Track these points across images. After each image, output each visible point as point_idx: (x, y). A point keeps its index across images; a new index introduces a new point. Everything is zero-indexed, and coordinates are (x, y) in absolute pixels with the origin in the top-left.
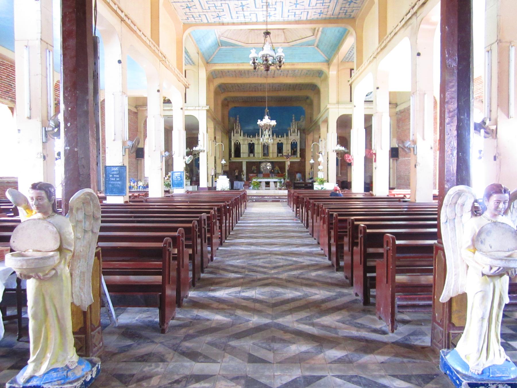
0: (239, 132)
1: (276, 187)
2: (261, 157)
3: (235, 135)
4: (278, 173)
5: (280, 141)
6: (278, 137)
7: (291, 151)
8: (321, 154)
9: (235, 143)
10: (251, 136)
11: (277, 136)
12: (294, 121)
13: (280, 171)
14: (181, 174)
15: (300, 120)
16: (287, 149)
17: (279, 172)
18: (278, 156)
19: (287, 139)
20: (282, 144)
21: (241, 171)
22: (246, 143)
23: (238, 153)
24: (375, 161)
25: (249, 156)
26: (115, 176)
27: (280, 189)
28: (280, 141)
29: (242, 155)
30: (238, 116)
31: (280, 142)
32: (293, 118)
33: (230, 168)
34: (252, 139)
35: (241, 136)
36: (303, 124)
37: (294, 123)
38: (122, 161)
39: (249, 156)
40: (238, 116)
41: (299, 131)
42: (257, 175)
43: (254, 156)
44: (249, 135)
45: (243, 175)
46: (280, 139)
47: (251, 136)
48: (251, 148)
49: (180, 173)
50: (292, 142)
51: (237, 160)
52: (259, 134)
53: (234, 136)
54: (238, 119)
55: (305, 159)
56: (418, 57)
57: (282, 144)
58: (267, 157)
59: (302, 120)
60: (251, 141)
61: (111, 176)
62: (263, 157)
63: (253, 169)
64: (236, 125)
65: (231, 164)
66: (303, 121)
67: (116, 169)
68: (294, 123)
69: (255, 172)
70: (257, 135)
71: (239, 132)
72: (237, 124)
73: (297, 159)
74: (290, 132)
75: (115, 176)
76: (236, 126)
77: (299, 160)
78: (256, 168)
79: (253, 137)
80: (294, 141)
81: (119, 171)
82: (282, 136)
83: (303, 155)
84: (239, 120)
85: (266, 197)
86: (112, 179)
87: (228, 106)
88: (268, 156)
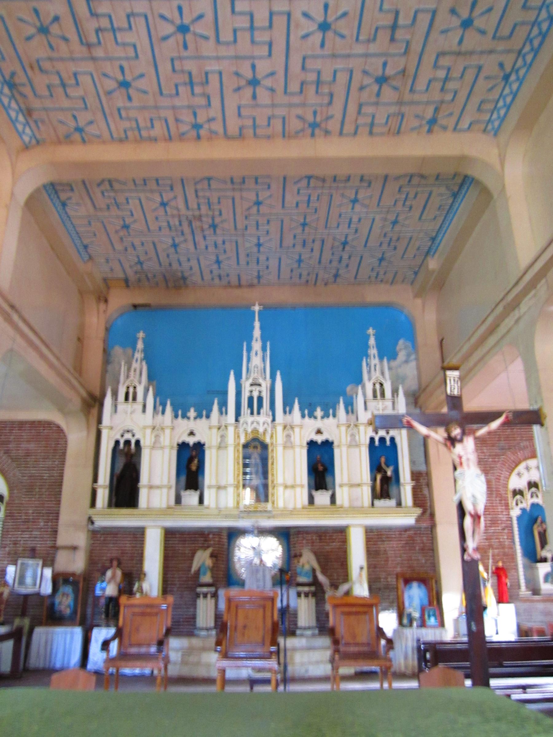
2: (231, 503)
3: (120, 407)
4: (315, 582)
5: (319, 432)
6: (312, 415)
7: (374, 479)
9: (117, 443)
10: (192, 413)
12: (373, 351)
13: (324, 572)
17: (321, 578)
20: (328, 445)
25: (178, 500)
28: (319, 432)
30: (141, 335)
31: (319, 439)
32: (372, 341)
33: (92, 560)
42: (215, 595)
43: (201, 501)
47: (192, 413)
52: (223, 404)
54: (140, 345)
57: (328, 445)
59: (402, 356)
60: (192, 433)
63: (195, 567)
64: (129, 369)
66: (406, 362)
70: (215, 407)
72: (135, 365)
78: (209, 562)
84: (145, 351)
87: (106, 301)
88: (267, 500)
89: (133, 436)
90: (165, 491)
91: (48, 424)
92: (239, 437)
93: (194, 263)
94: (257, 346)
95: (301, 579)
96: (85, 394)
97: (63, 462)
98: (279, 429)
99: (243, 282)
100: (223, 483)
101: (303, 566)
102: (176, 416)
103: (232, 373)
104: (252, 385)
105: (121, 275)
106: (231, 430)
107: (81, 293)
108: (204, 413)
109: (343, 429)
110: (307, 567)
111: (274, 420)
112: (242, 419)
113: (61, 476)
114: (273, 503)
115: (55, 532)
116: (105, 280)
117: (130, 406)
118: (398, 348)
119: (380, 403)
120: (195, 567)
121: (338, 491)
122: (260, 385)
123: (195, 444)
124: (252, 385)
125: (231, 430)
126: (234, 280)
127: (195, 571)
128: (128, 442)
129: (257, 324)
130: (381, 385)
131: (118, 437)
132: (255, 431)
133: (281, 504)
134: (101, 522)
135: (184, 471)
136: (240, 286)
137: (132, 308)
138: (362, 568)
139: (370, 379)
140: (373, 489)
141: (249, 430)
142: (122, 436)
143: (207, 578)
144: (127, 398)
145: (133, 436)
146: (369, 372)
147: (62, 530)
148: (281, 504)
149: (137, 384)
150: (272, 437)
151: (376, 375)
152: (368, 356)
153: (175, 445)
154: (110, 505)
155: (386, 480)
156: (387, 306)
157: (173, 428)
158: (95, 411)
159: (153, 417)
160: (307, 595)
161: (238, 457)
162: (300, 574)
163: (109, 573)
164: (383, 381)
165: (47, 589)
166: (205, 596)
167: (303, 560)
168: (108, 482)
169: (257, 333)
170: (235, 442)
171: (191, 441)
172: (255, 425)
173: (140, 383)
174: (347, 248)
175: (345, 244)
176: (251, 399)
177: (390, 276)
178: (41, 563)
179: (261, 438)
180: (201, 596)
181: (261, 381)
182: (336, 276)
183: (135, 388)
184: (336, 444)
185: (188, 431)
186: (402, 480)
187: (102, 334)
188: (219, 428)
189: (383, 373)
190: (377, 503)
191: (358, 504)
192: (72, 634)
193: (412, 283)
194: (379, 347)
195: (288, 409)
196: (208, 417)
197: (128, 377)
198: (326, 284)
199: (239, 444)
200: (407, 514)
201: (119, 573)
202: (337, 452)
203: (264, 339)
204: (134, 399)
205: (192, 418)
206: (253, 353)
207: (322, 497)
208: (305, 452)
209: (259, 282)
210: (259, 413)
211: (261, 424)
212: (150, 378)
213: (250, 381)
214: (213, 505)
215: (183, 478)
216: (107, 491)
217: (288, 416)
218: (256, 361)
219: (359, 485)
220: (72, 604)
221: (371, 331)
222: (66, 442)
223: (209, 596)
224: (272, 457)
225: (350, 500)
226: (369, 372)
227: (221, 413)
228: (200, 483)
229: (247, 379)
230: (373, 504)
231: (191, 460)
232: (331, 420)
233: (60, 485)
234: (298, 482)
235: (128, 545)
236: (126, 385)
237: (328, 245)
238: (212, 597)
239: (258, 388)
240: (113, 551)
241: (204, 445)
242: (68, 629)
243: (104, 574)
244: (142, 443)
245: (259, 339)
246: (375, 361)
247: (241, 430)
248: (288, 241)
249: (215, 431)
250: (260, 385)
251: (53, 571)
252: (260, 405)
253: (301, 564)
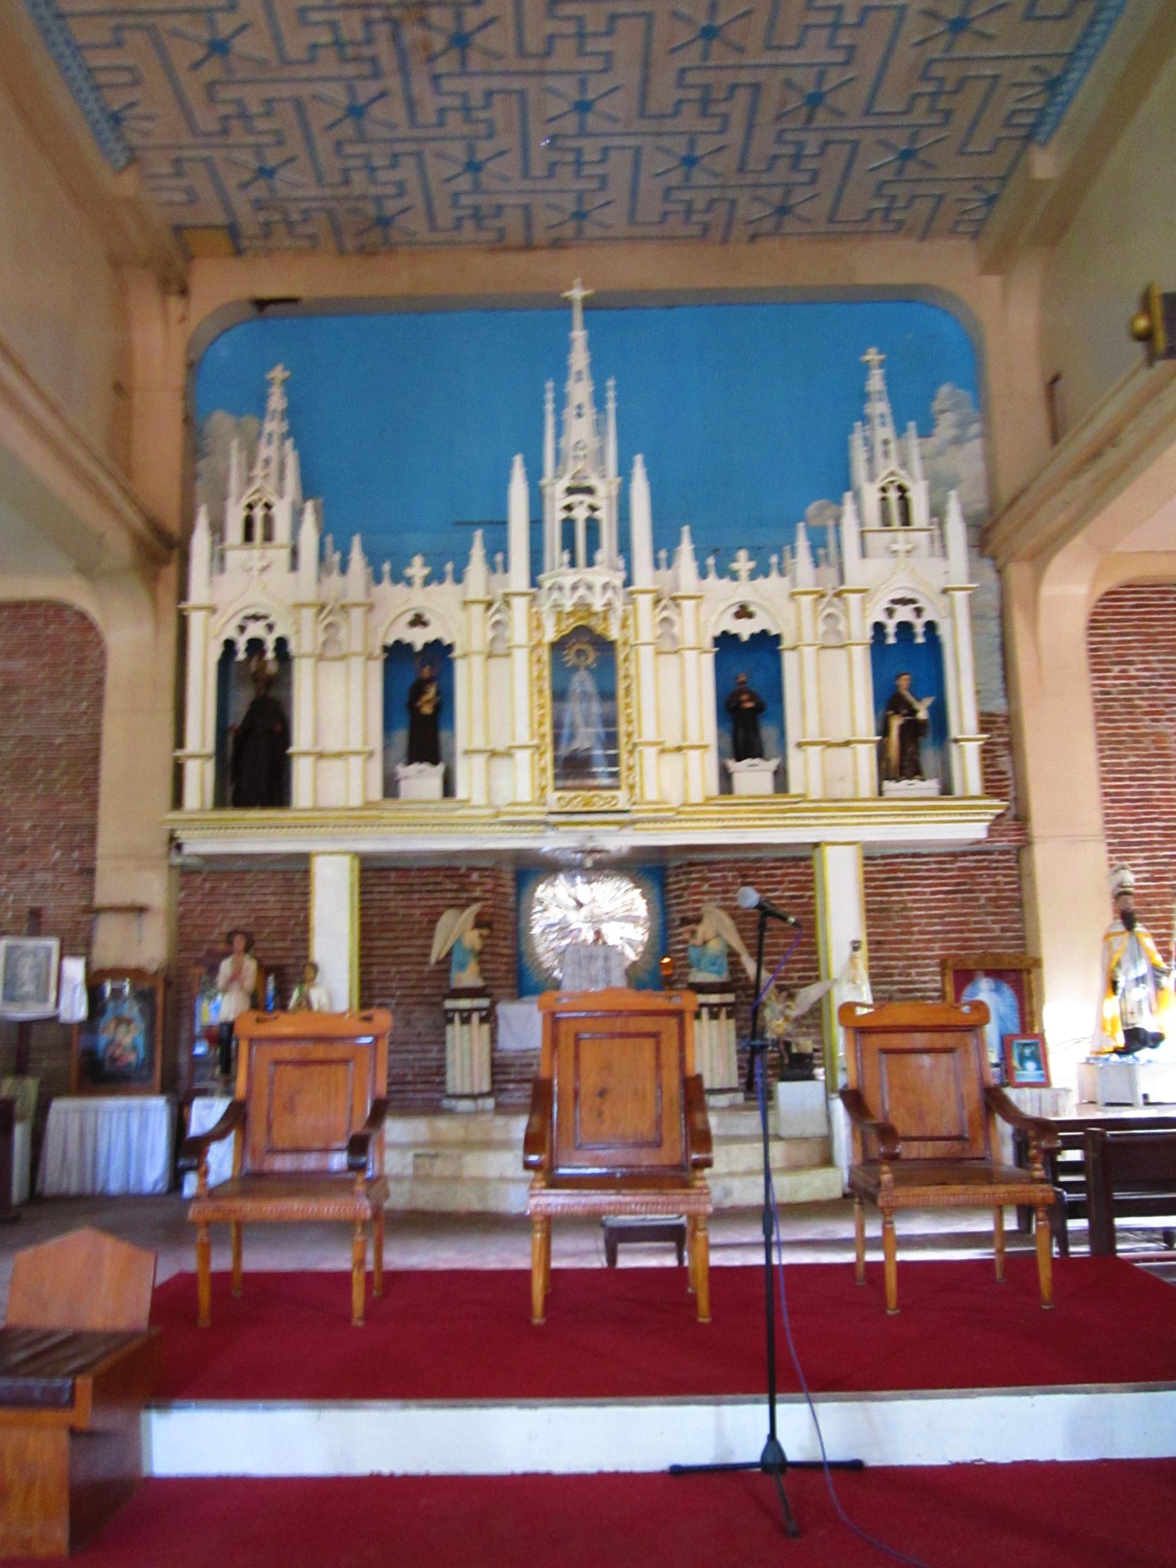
2: (525, 794)
5: (743, 612)
7: (883, 730)
9: (229, 645)
10: (418, 569)
12: (879, 408)
18: (726, 781)
22: (357, 645)
25: (391, 787)
29: (302, 773)
30: (278, 373)
31: (745, 629)
32: (876, 382)
34: (419, 598)
35: (294, 566)
39: (391, 787)
42: (489, 1017)
43: (448, 789)
47: (418, 569)
54: (277, 401)
58: (600, 800)
59: (945, 427)
60: (418, 621)
62: (552, 796)
63: (437, 951)
66: (957, 441)
69: (468, 977)
70: (477, 553)
72: (266, 451)
74: (859, 514)
77: (976, 831)
78: (473, 939)
79: (435, 577)
80: (904, 614)
84: (289, 413)
87: (184, 292)
89: (270, 627)
90: (356, 762)
91: (56, 610)
92: (539, 626)
93: (407, 171)
94: (580, 391)
96: (137, 522)
97: (98, 703)
98: (645, 601)
99: (540, 235)
100: (501, 746)
101: (705, 943)
102: (377, 578)
103: (518, 460)
104: (571, 491)
105: (220, 219)
106: (520, 604)
107: (116, 263)
108: (449, 567)
109: (806, 600)
110: (714, 947)
111: (628, 582)
112: (546, 580)
113: (96, 737)
114: (632, 787)
115: (89, 872)
116: (178, 229)
117: (256, 553)
118: (937, 405)
119: (901, 536)
120: (437, 951)
121: (795, 759)
122: (589, 491)
123: (427, 646)
124: (571, 491)
125: (520, 605)
126: (512, 222)
127: (438, 962)
128: (255, 646)
129: (579, 335)
130: (902, 489)
131: (231, 632)
132: (583, 607)
133: (651, 794)
134: (198, 844)
135: (404, 718)
136: (528, 246)
137: (251, 310)
138: (856, 946)
139: (872, 478)
140: (882, 750)
141: (568, 605)
142: (242, 629)
143: (468, 977)
144: (248, 536)
145: (270, 627)
146: (870, 460)
147: (103, 866)
148: (651, 794)
149: (273, 499)
150: (624, 626)
152: (866, 420)
153: (378, 651)
154: (220, 802)
155: (913, 732)
156: (908, 295)
157: (370, 607)
158: (170, 573)
159: (319, 580)
161: (540, 677)
162: (698, 965)
163: (226, 967)
164: (907, 483)
165: (75, 1008)
166: (466, 1021)
167: (704, 930)
168: (210, 746)
169: (579, 359)
170: (530, 639)
171: (419, 638)
172: (582, 591)
173: (281, 493)
174: (822, 117)
175: (815, 100)
176: (568, 526)
177: (923, 207)
178: (53, 944)
179: (599, 628)
180: (457, 1017)
181: (593, 481)
182: (783, 210)
183: (268, 506)
184: (786, 643)
185: (409, 617)
186: (954, 732)
187: (176, 374)
188: (489, 605)
189: (904, 464)
190: (888, 785)
191: (844, 790)
192: (144, 1111)
193: (975, 236)
194: (893, 392)
195: (663, 554)
196: (459, 579)
197: (250, 480)
198: (753, 238)
199: (539, 645)
200: (968, 812)
202: (789, 661)
203: (598, 372)
204: (268, 537)
205: (418, 581)
206: (570, 411)
208: (708, 661)
209: (579, 231)
210: (590, 563)
211: (598, 589)
212: (308, 490)
213: (566, 482)
214: (479, 799)
215: (401, 737)
216: (210, 767)
217: (664, 573)
218: (580, 429)
219: (847, 744)
220: (141, 1042)
222: (103, 655)
223: (475, 1017)
224: (626, 677)
225: (825, 782)
226: (870, 460)
227: (492, 568)
228: (444, 751)
229: (558, 476)
230: (881, 793)
231: (418, 689)
232: (773, 584)
233: (95, 760)
234: (693, 738)
235: (272, 904)
236: (245, 501)
237: (769, 105)
238: (483, 1020)
239: (587, 499)
240: (235, 916)
241: (450, 648)
242: (135, 1102)
243: (214, 970)
244: (292, 647)
245: (586, 375)
246: (885, 432)
247: (546, 606)
248: (664, 93)
249: (478, 610)
250: (589, 491)
251: (88, 966)
252: (593, 543)
253: (698, 941)
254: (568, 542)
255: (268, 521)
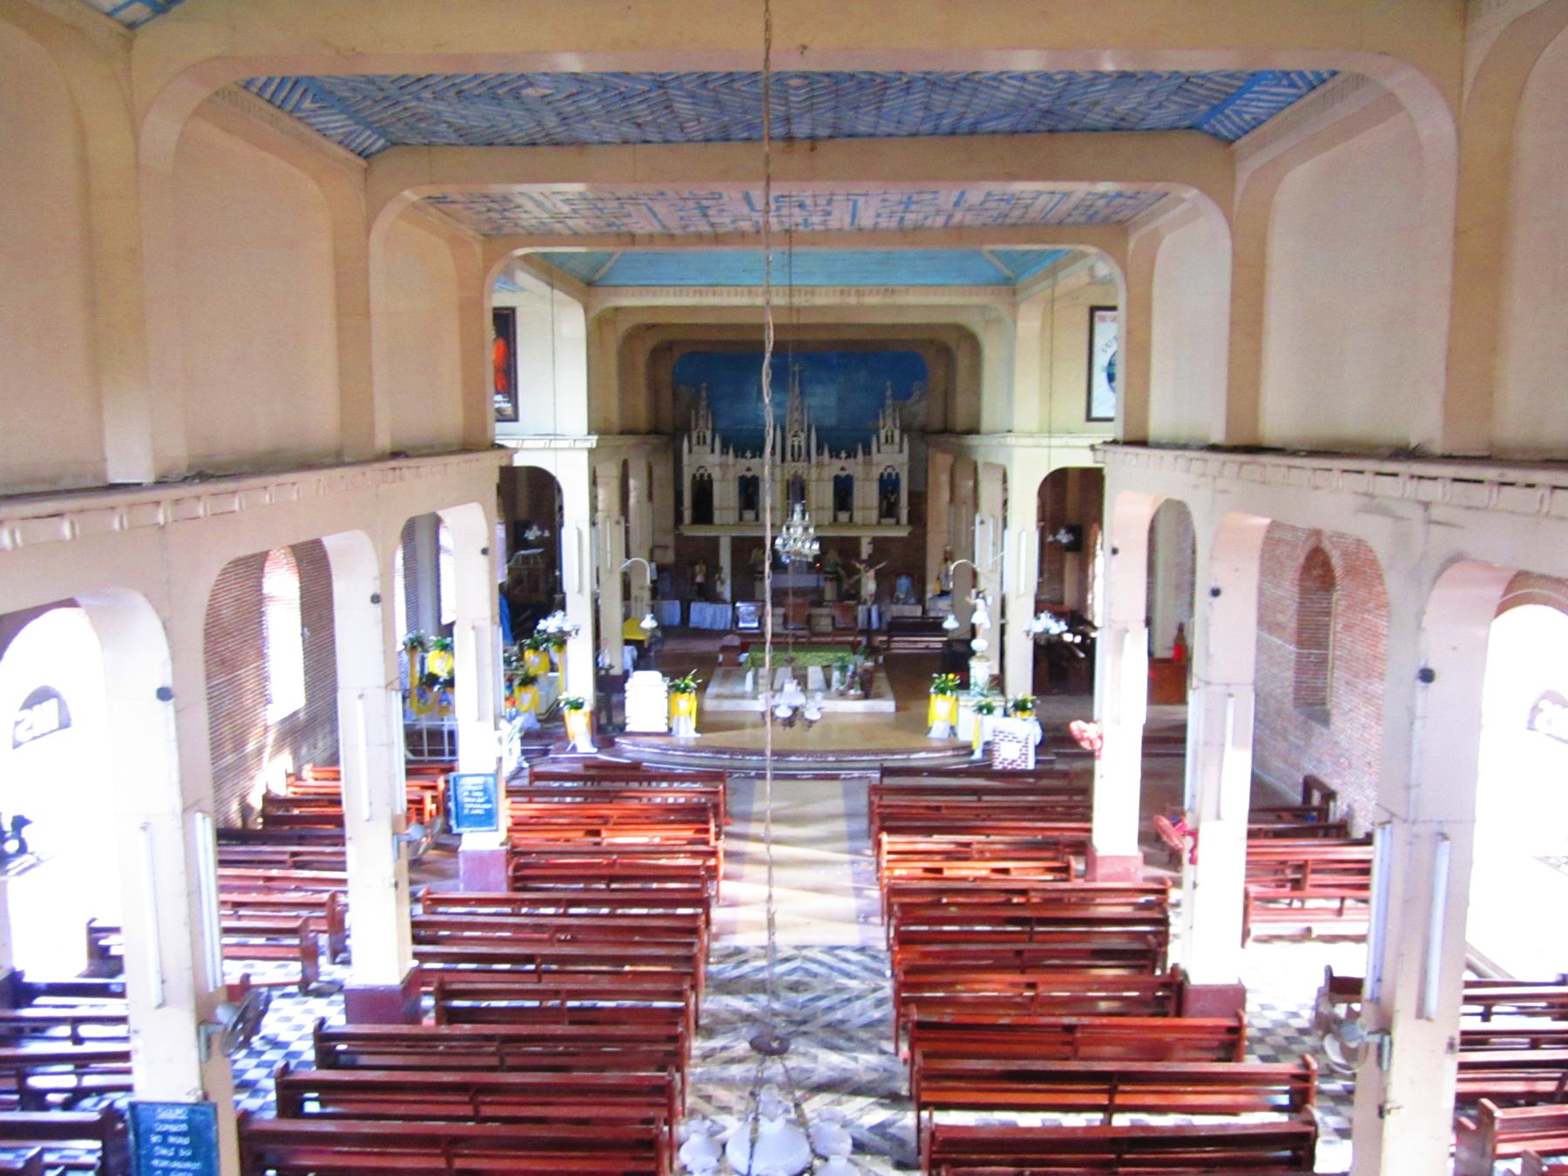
0: (709, 441)
1: (828, 683)
3: (695, 448)
6: (838, 456)
8: (984, 598)
9: (694, 476)
10: (748, 454)
11: (835, 454)
14: (485, 783)
15: (909, 395)
16: (866, 496)
19: (868, 464)
21: (713, 569)
23: (703, 511)
24: (1193, 861)
25: (741, 518)
26: (172, 1139)
27: (842, 695)
31: (843, 474)
32: (889, 393)
33: (678, 554)
35: (713, 451)
36: (922, 409)
37: (889, 411)
38: (196, 1083)
40: (704, 385)
41: (906, 440)
43: (757, 518)
44: (740, 453)
45: (723, 583)
46: (842, 463)
47: (748, 454)
48: (749, 492)
49: (480, 780)
50: (882, 475)
51: (702, 531)
53: (690, 451)
55: (925, 526)
56: (1421, 684)
60: (749, 469)
61: (155, 1139)
64: (697, 413)
65: (682, 542)
66: (919, 401)
67: (179, 1113)
68: (889, 411)
71: (709, 441)
72: (702, 412)
73: (899, 532)
75: (172, 1139)
76: (697, 419)
79: (754, 456)
80: (889, 470)
81: (188, 1122)
82: (851, 454)
83: (918, 518)
85: (793, 758)
86: (164, 1152)
95: (828, 569)
128: (702, 475)
144: (698, 443)
151: (889, 422)
160: (831, 580)
176: (793, 446)
190: (884, 521)
191: (867, 522)
201: (704, 568)
204: (705, 442)
207: (843, 517)
221: (889, 383)
232: (851, 460)
244: (713, 476)
252: (800, 455)
254: (793, 455)
255: (704, 437)
